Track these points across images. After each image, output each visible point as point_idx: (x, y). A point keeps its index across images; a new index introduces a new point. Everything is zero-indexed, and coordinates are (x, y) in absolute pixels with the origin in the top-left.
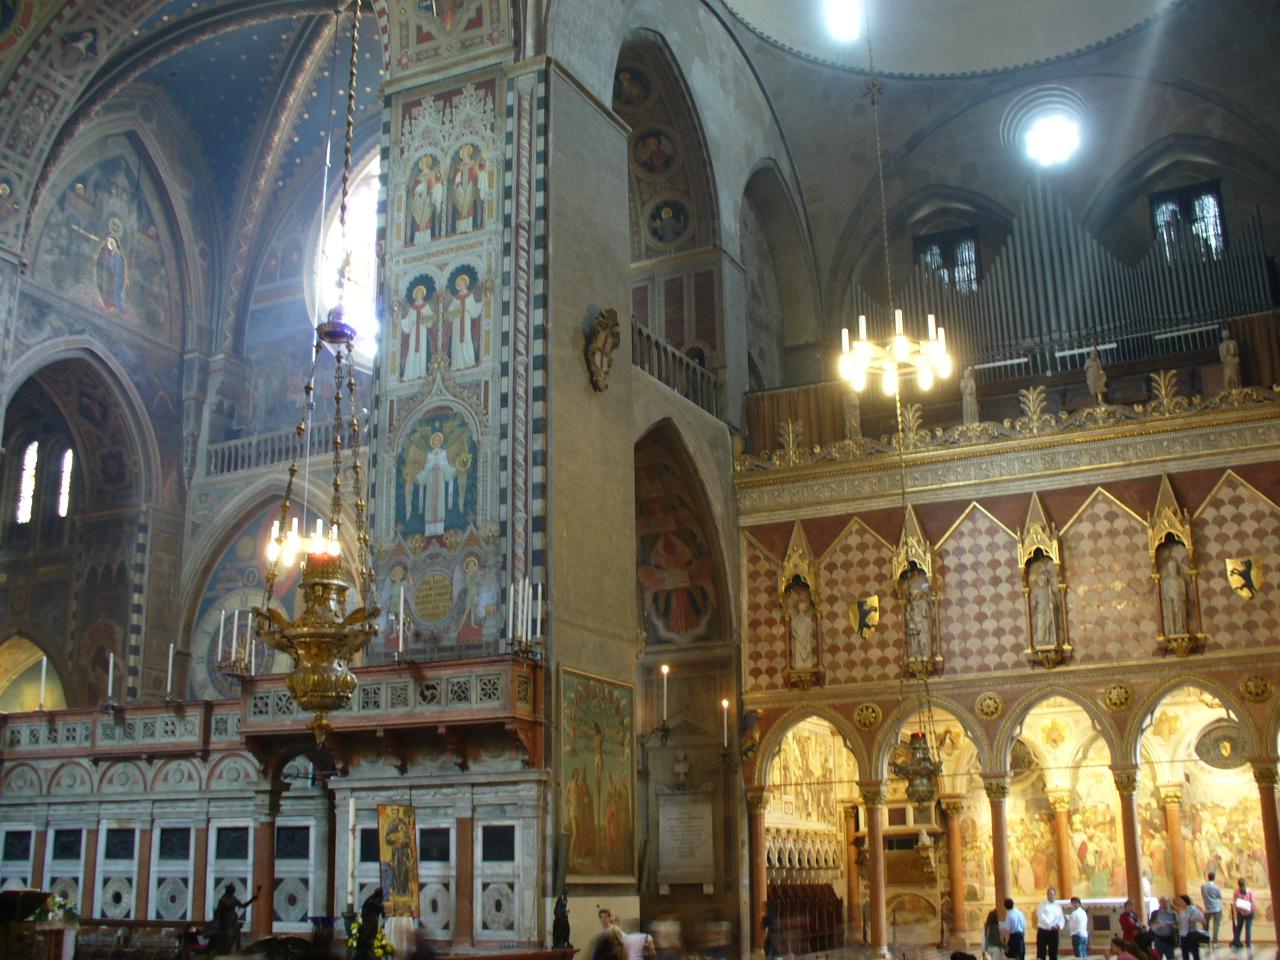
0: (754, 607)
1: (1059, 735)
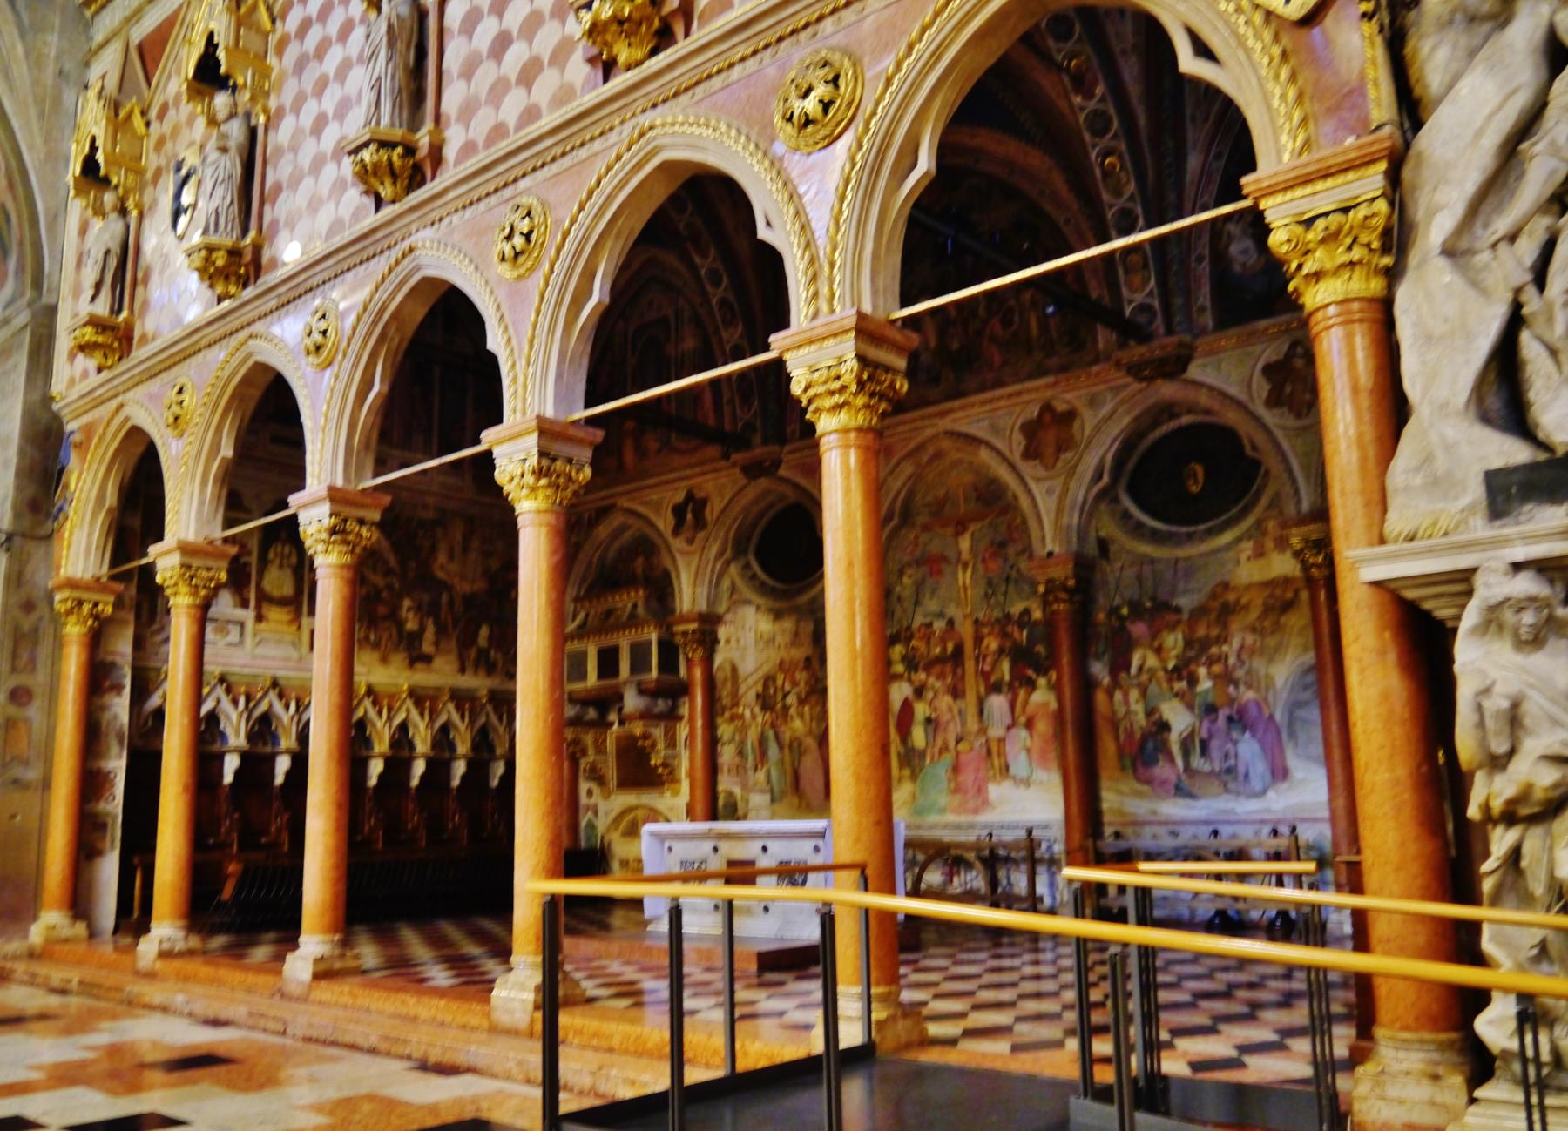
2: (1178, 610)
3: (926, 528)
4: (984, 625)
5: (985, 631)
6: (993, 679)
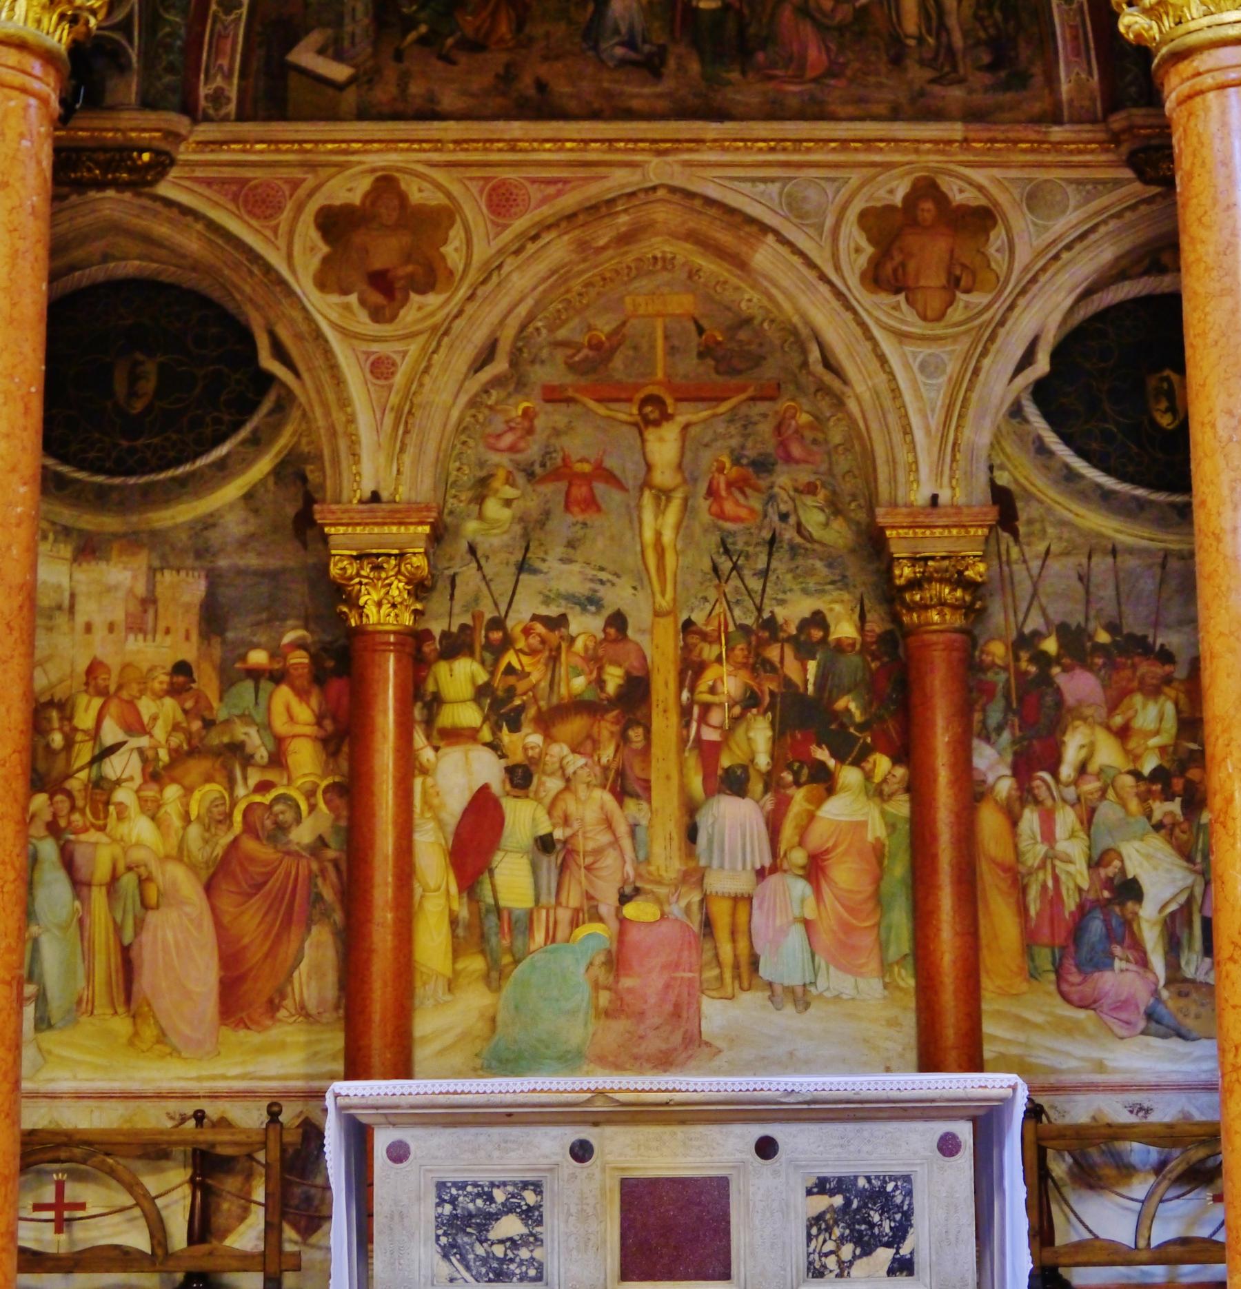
2: (1166, 656)
3: (553, 395)
4: (704, 636)
5: (709, 652)
6: (726, 761)
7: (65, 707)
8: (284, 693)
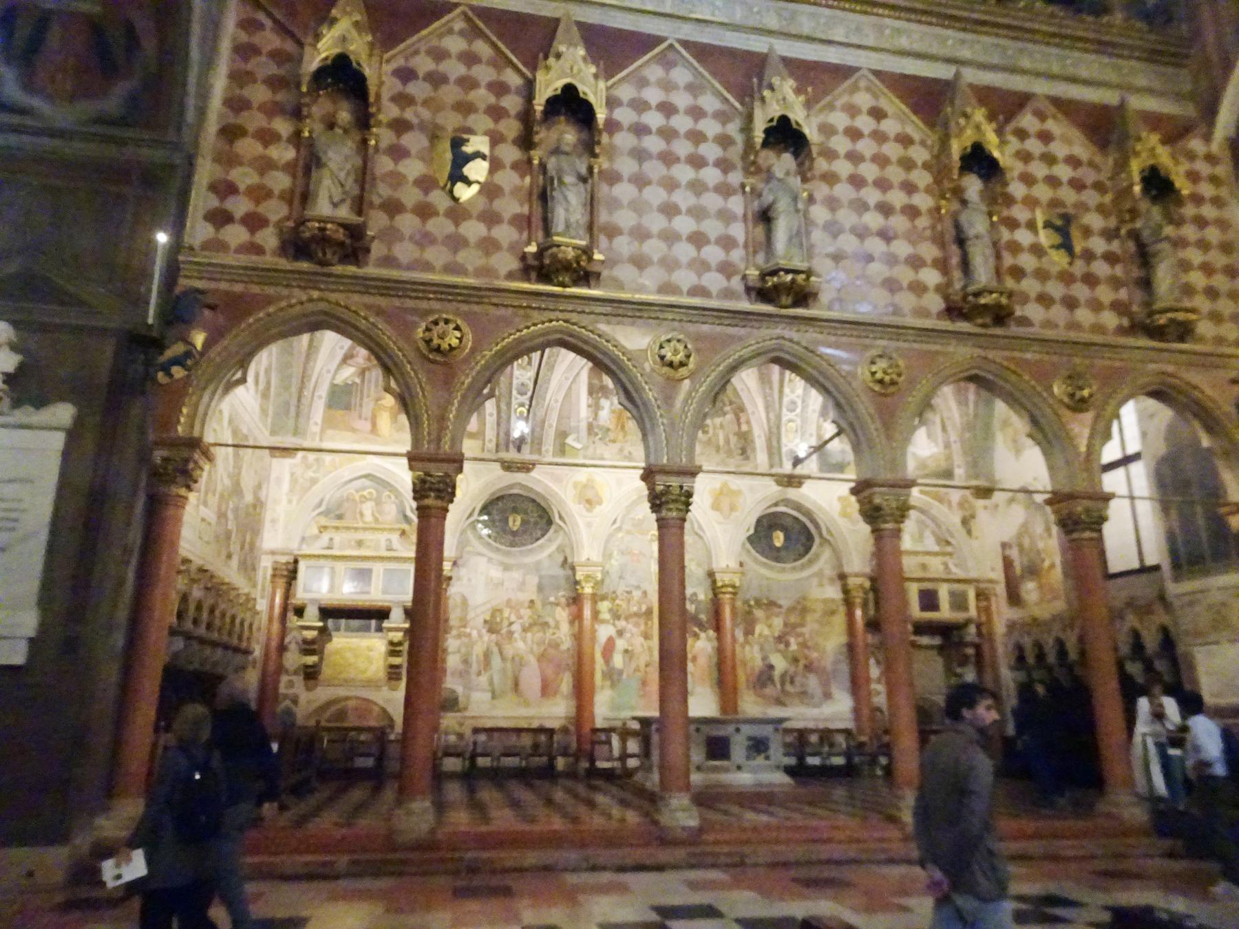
0: (236, 104)
1: (597, 495)
2: (780, 607)
3: (628, 532)
7: (500, 611)
8: (559, 609)
